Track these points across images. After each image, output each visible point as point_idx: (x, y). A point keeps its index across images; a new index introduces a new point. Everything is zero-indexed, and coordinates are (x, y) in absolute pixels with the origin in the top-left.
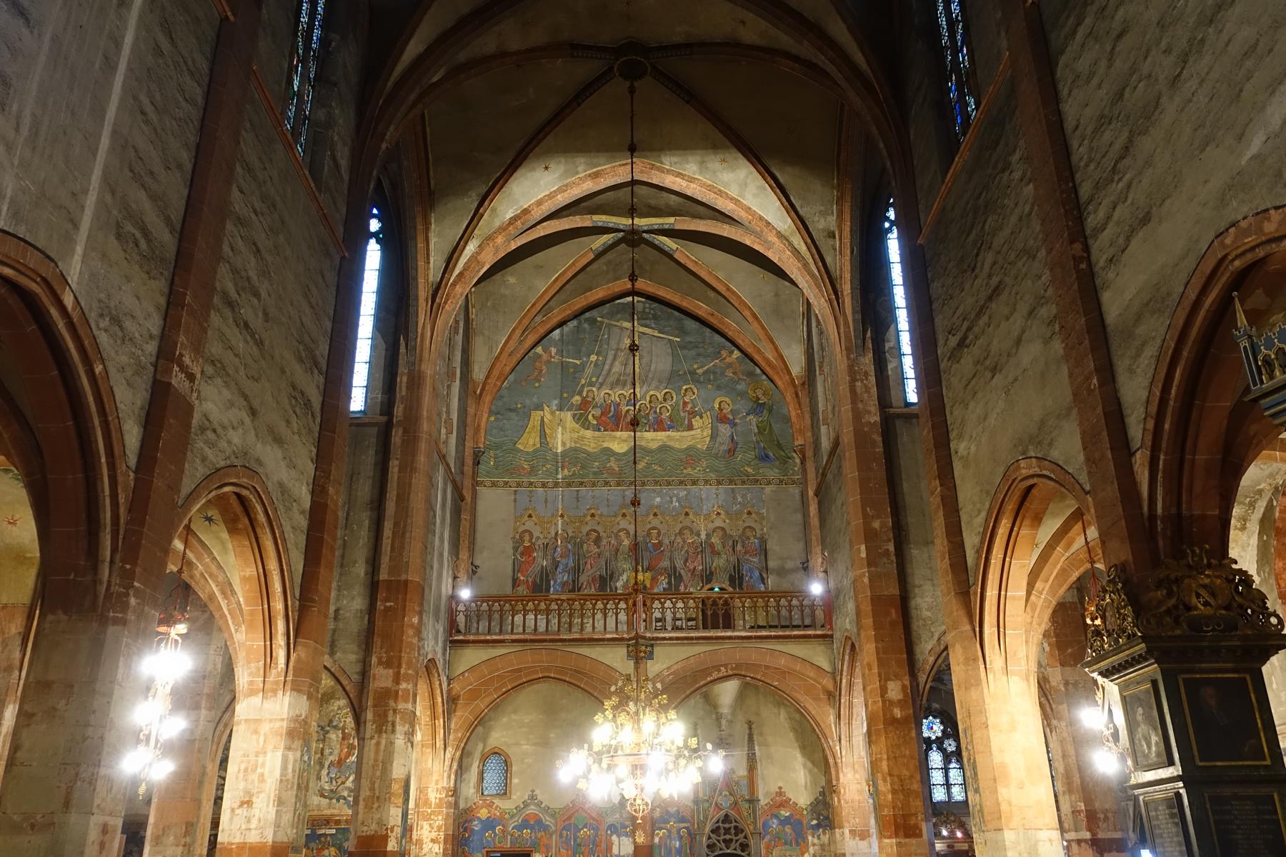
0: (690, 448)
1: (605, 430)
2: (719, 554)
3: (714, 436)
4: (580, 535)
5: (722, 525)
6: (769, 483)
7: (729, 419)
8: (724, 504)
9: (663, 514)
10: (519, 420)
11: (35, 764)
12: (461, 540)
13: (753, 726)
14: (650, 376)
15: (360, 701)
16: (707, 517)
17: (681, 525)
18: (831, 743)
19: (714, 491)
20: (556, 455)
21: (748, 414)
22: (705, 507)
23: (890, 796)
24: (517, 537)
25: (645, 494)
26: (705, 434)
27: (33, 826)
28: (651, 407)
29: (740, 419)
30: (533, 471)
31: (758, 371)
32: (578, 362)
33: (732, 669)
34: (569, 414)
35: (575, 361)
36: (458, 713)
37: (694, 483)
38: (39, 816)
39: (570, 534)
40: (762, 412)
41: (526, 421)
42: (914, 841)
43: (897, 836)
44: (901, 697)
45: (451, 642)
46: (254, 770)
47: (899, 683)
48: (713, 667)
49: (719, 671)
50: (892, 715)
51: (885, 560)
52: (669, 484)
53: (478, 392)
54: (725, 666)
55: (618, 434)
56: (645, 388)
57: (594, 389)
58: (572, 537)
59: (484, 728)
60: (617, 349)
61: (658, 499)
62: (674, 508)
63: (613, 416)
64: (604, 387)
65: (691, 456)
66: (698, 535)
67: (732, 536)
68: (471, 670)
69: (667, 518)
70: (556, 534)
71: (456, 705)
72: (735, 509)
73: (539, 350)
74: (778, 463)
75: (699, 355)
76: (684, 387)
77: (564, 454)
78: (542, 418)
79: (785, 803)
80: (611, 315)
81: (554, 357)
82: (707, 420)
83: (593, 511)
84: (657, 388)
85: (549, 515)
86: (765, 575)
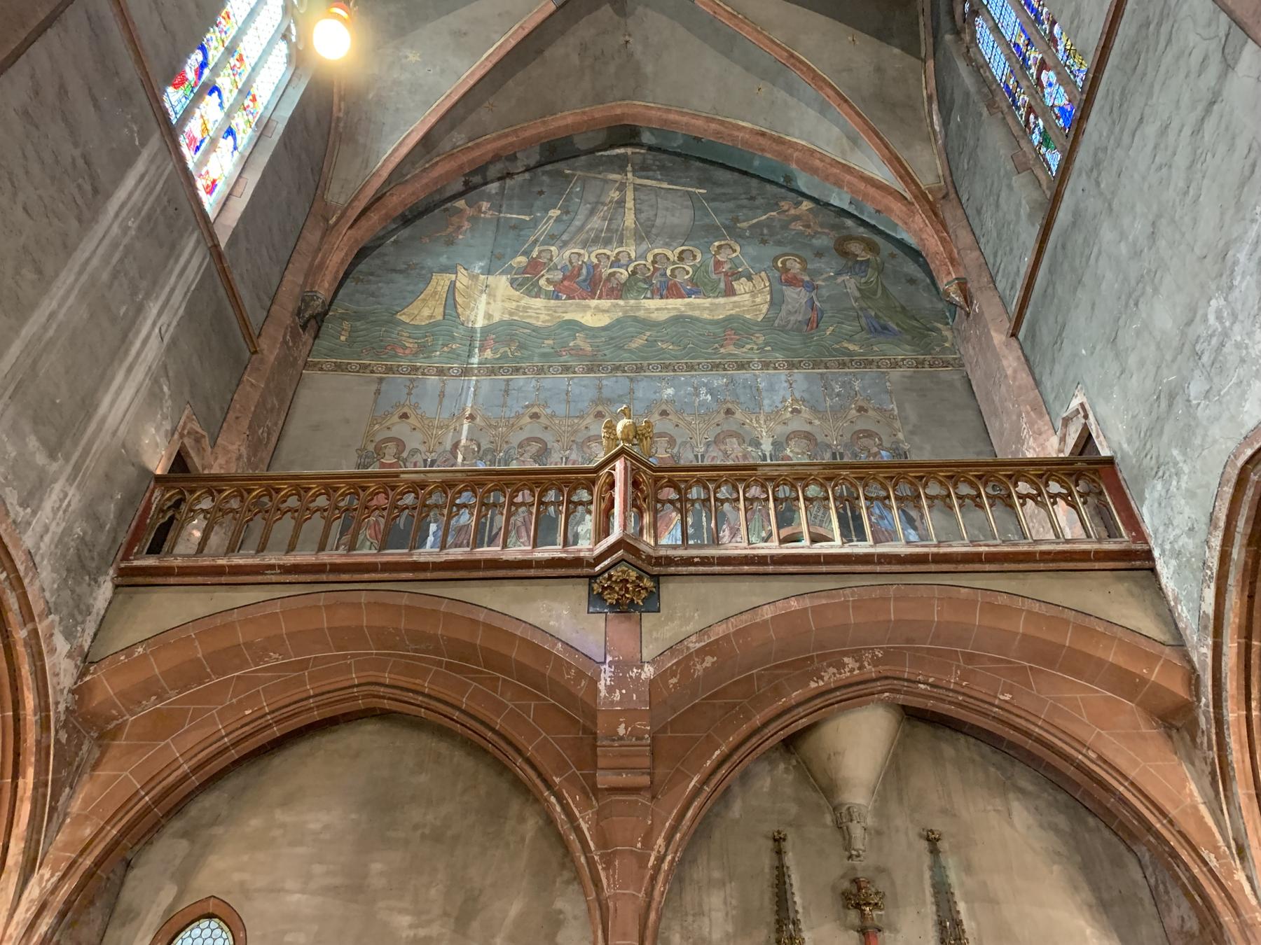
0: (729, 319)
1: (569, 298)
3: (776, 302)
4: (505, 447)
5: (808, 428)
6: (895, 365)
7: (802, 281)
8: (806, 396)
9: (679, 412)
10: (408, 284)
12: (231, 415)
13: (943, 845)
14: (654, 231)
16: (775, 414)
17: (718, 430)
18: (1213, 863)
19: (783, 378)
20: (473, 330)
21: (839, 274)
22: (766, 402)
24: (371, 447)
25: (643, 384)
26: (758, 300)
28: (656, 269)
29: (824, 280)
30: (424, 349)
31: (849, 223)
32: (527, 218)
33: (876, 662)
34: (504, 278)
35: (523, 217)
36: (103, 773)
37: (742, 366)
39: (485, 445)
40: (865, 271)
41: (421, 286)
45: (122, 572)
48: (822, 657)
49: (840, 666)
52: (691, 368)
53: (331, 222)
54: (857, 655)
55: (594, 303)
56: (644, 246)
57: (553, 248)
58: (487, 451)
59: (193, 842)
60: (597, 203)
61: (670, 391)
62: (702, 404)
63: (585, 281)
64: (572, 245)
65: (735, 328)
66: (756, 444)
67: (829, 446)
68: (159, 641)
69: (689, 419)
70: (456, 445)
71: (103, 754)
72: (829, 402)
73: (461, 203)
74: (909, 337)
75: (741, 207)
76: (716, 244)
77: (486, 330)
78: (452, 286)
80: (591, 167)
81: (485, 213)
82: (762, 283)
83: (535, 410)
84: (667, 245)
85: (446, 415)
86: (914, 514)
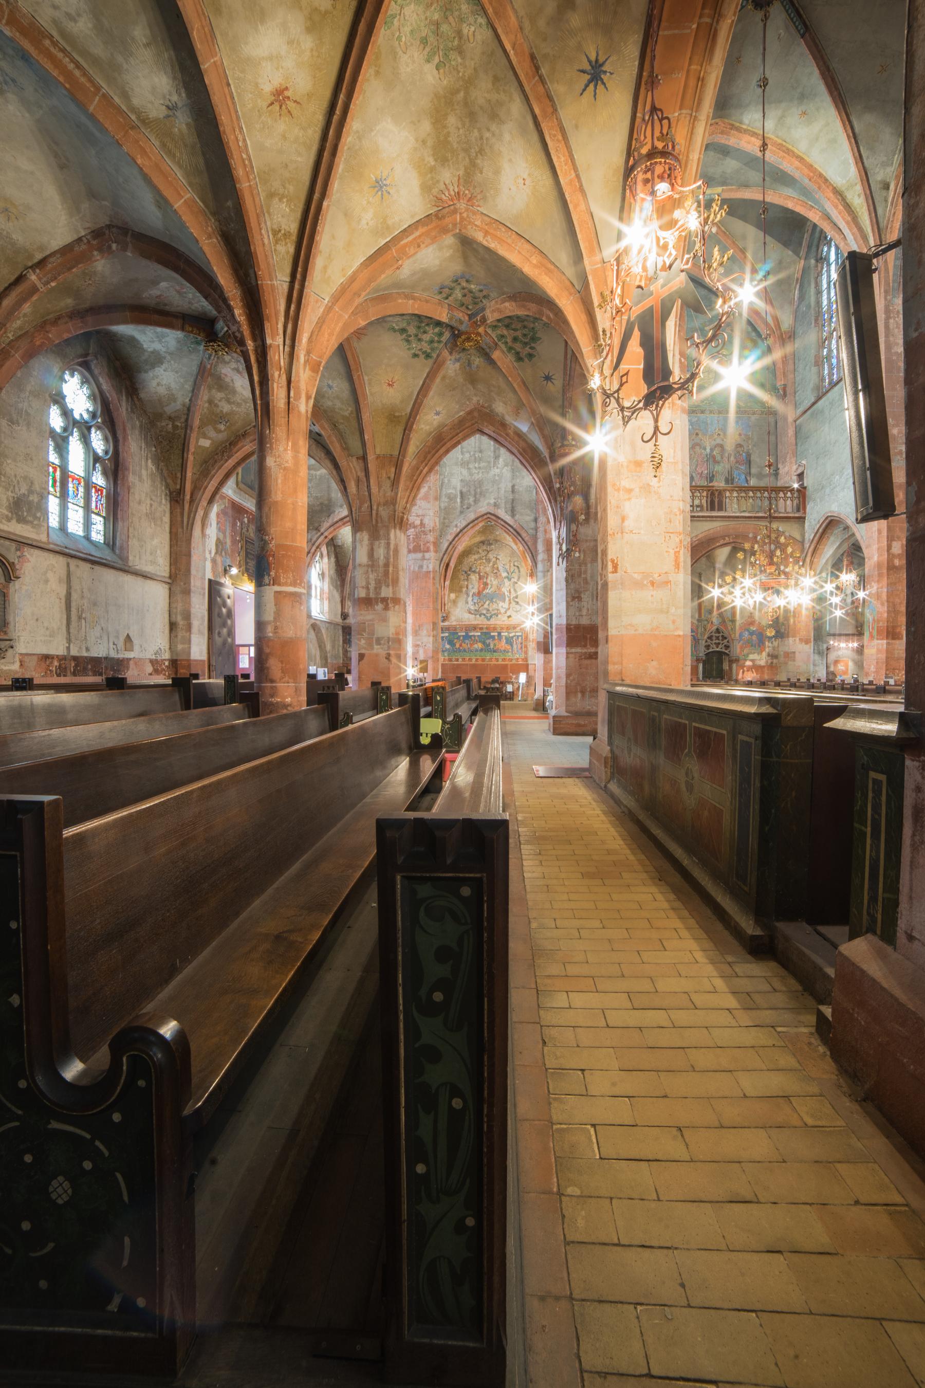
2: (718, 462)
11: (642, 532)
15: (536, 548)
23: (886, 615)
27: (652, 583)
37: (702, 412)
38: (656, 576)
42: (897, 642)
43: (887, 638)
44: (900, 552)
46: (580, 575)
47: (900, 543)
50: (893, 563)
51: (899, 457)
54: (728, 536)
66: (705, 449)
79: (752, 623)
